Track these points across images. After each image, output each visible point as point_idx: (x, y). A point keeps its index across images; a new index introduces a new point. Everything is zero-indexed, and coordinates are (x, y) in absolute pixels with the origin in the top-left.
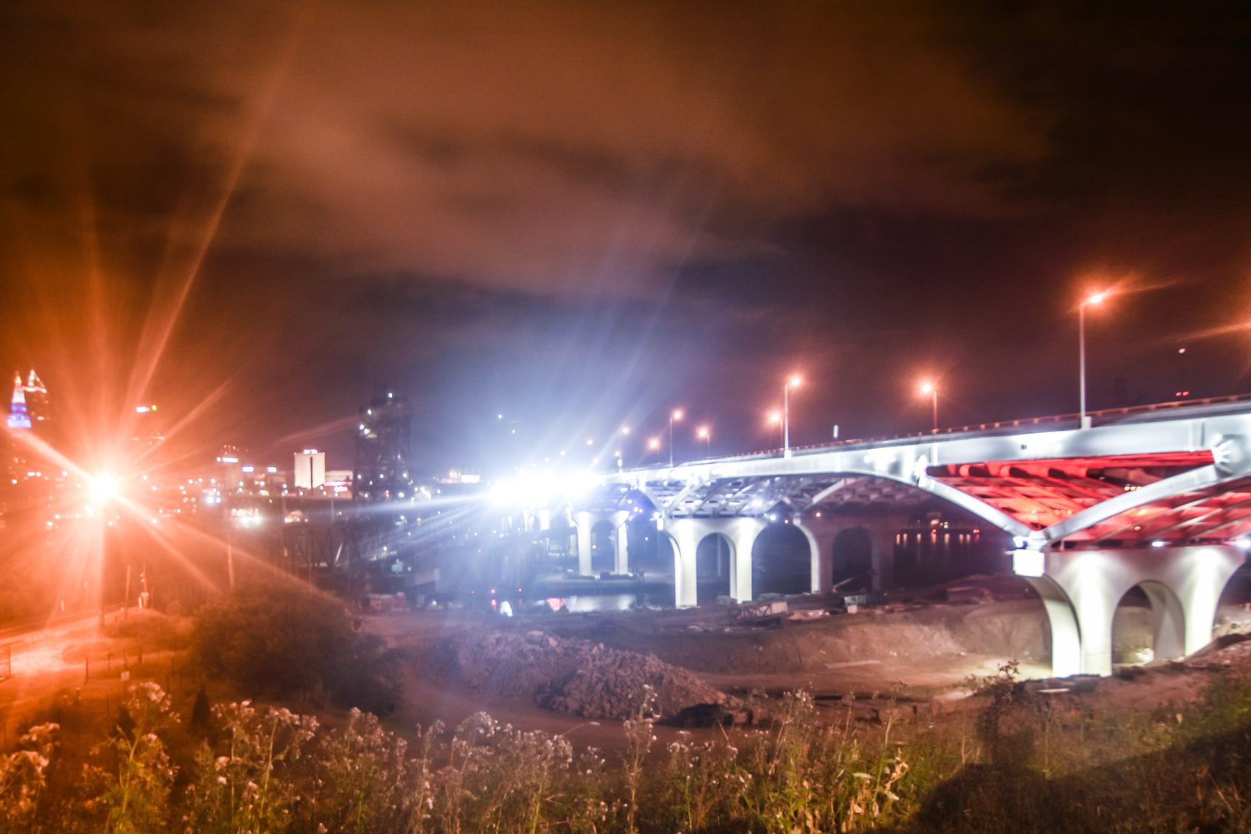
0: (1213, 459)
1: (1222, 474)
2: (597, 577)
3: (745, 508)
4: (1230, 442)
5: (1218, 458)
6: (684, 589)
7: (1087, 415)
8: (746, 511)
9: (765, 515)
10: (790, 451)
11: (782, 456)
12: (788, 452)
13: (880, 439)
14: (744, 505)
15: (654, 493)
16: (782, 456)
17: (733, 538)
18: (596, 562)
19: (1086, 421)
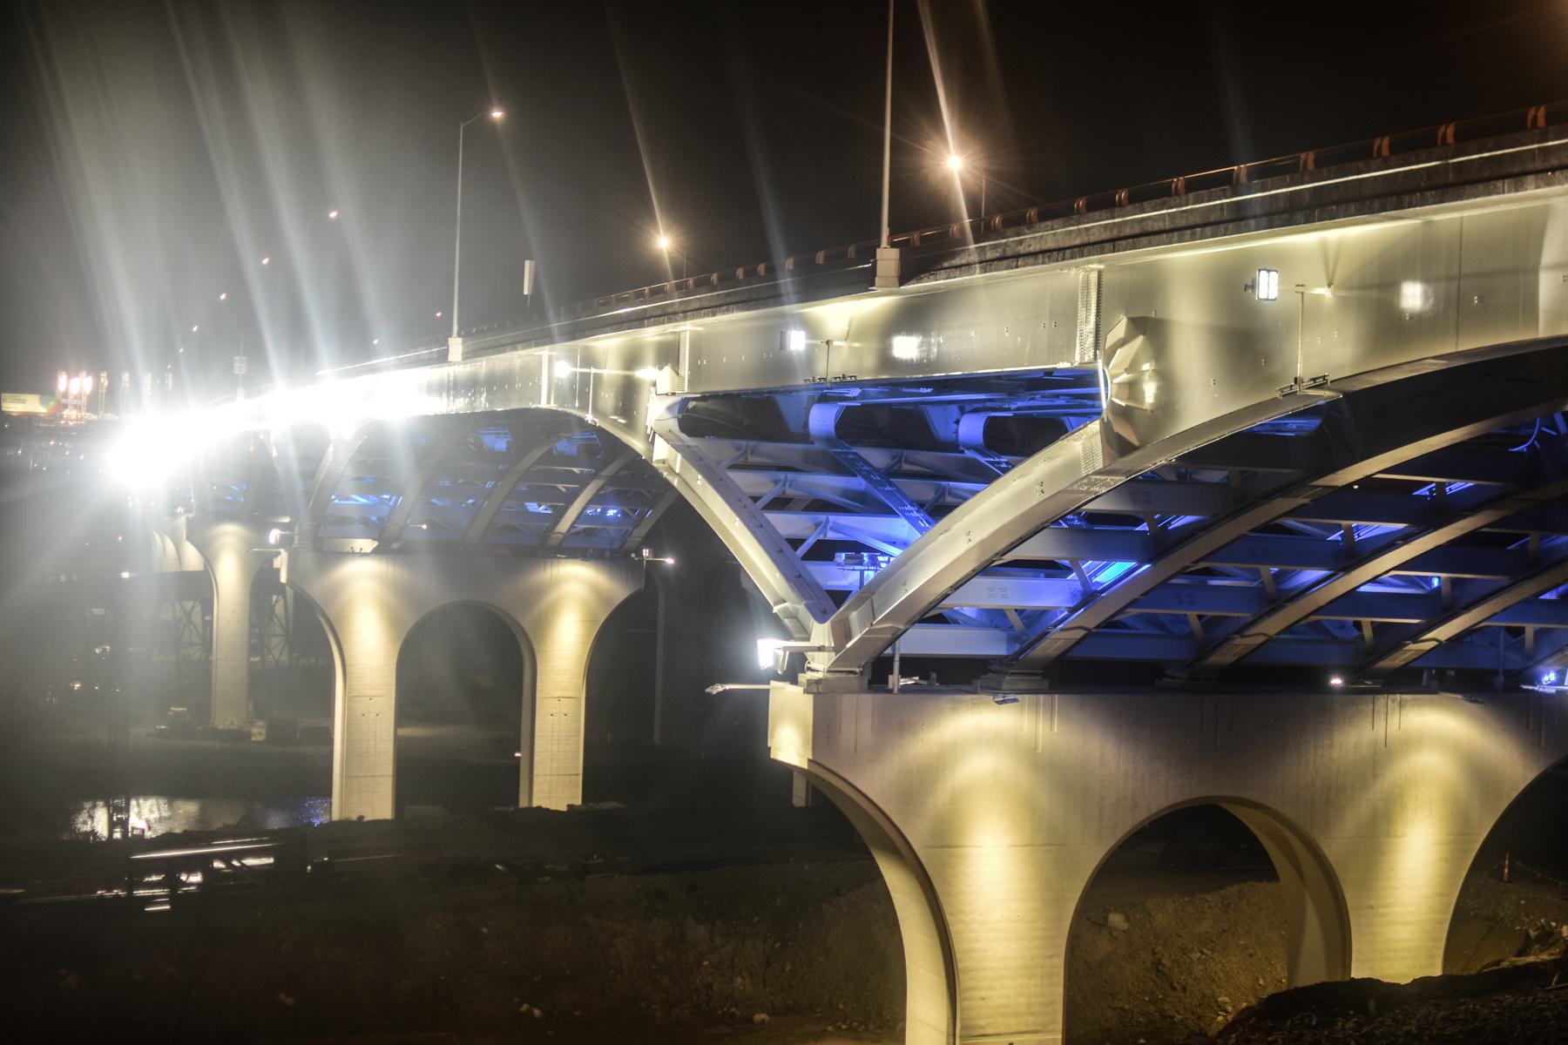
0: (1095, 397)
1: (1118, 446)
2: (259, 733)
3: (564, 525)
4: (1141, 338)
5: (1109, 394)
6: (347, 776)
7: (893, 245)
8: (572, 533)
9: (646, 552)
10: (460, 340)
11: (442, 358)
12: (456, 346)
13: (608, 305)
14: (559, 514)
15: (747, 481)
16: (442, 358)
17: (526, 626)
18: (259, 682)
19: (888, 258)
